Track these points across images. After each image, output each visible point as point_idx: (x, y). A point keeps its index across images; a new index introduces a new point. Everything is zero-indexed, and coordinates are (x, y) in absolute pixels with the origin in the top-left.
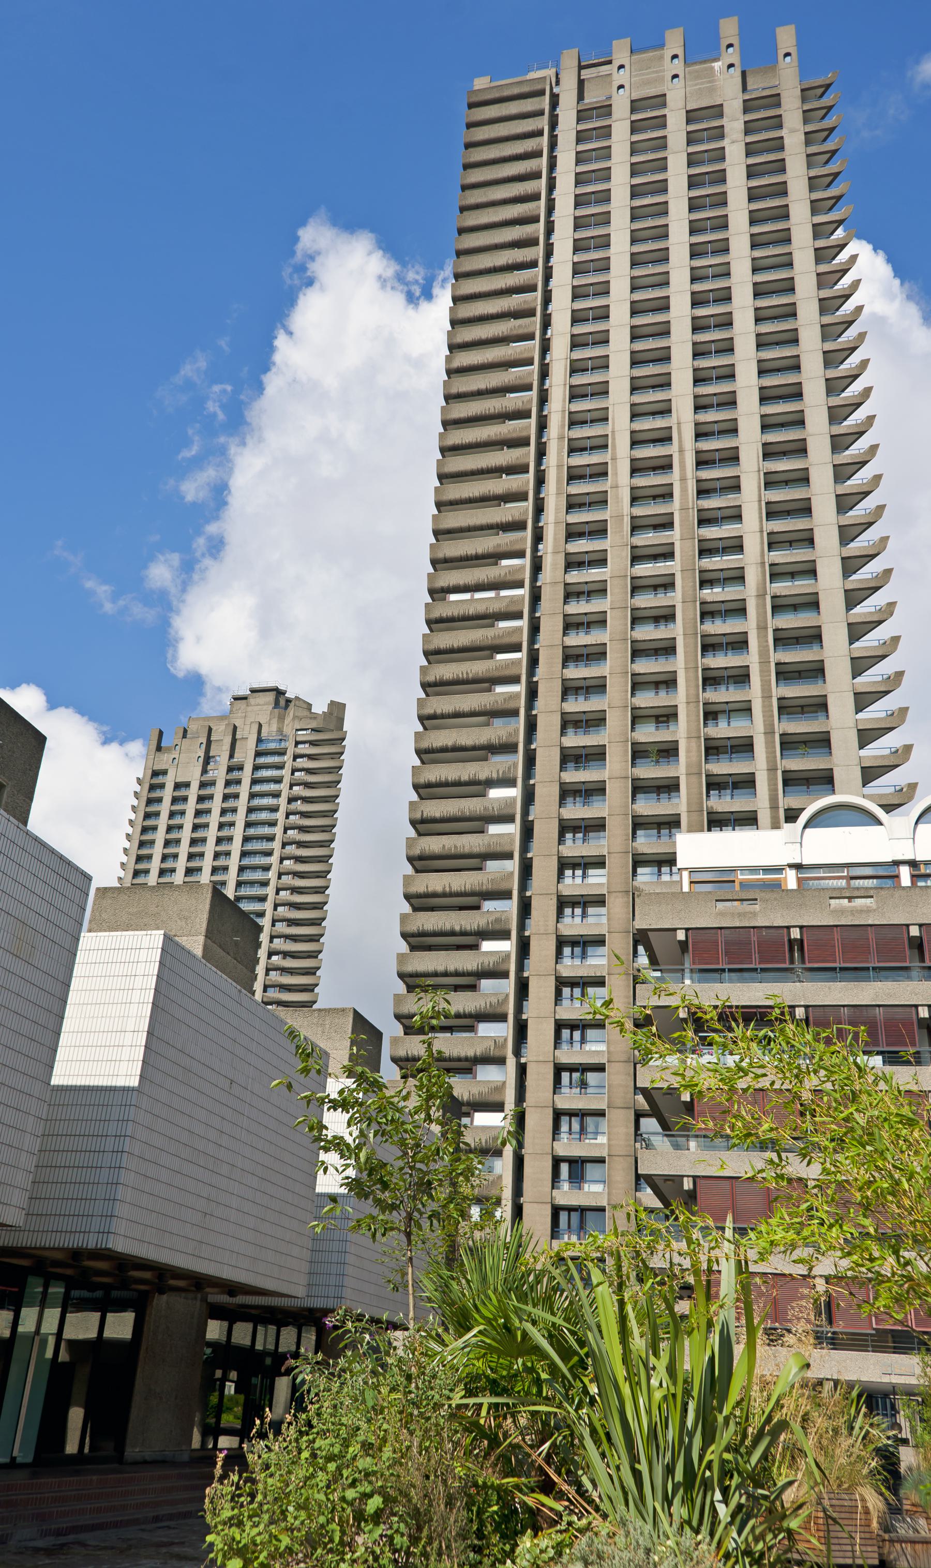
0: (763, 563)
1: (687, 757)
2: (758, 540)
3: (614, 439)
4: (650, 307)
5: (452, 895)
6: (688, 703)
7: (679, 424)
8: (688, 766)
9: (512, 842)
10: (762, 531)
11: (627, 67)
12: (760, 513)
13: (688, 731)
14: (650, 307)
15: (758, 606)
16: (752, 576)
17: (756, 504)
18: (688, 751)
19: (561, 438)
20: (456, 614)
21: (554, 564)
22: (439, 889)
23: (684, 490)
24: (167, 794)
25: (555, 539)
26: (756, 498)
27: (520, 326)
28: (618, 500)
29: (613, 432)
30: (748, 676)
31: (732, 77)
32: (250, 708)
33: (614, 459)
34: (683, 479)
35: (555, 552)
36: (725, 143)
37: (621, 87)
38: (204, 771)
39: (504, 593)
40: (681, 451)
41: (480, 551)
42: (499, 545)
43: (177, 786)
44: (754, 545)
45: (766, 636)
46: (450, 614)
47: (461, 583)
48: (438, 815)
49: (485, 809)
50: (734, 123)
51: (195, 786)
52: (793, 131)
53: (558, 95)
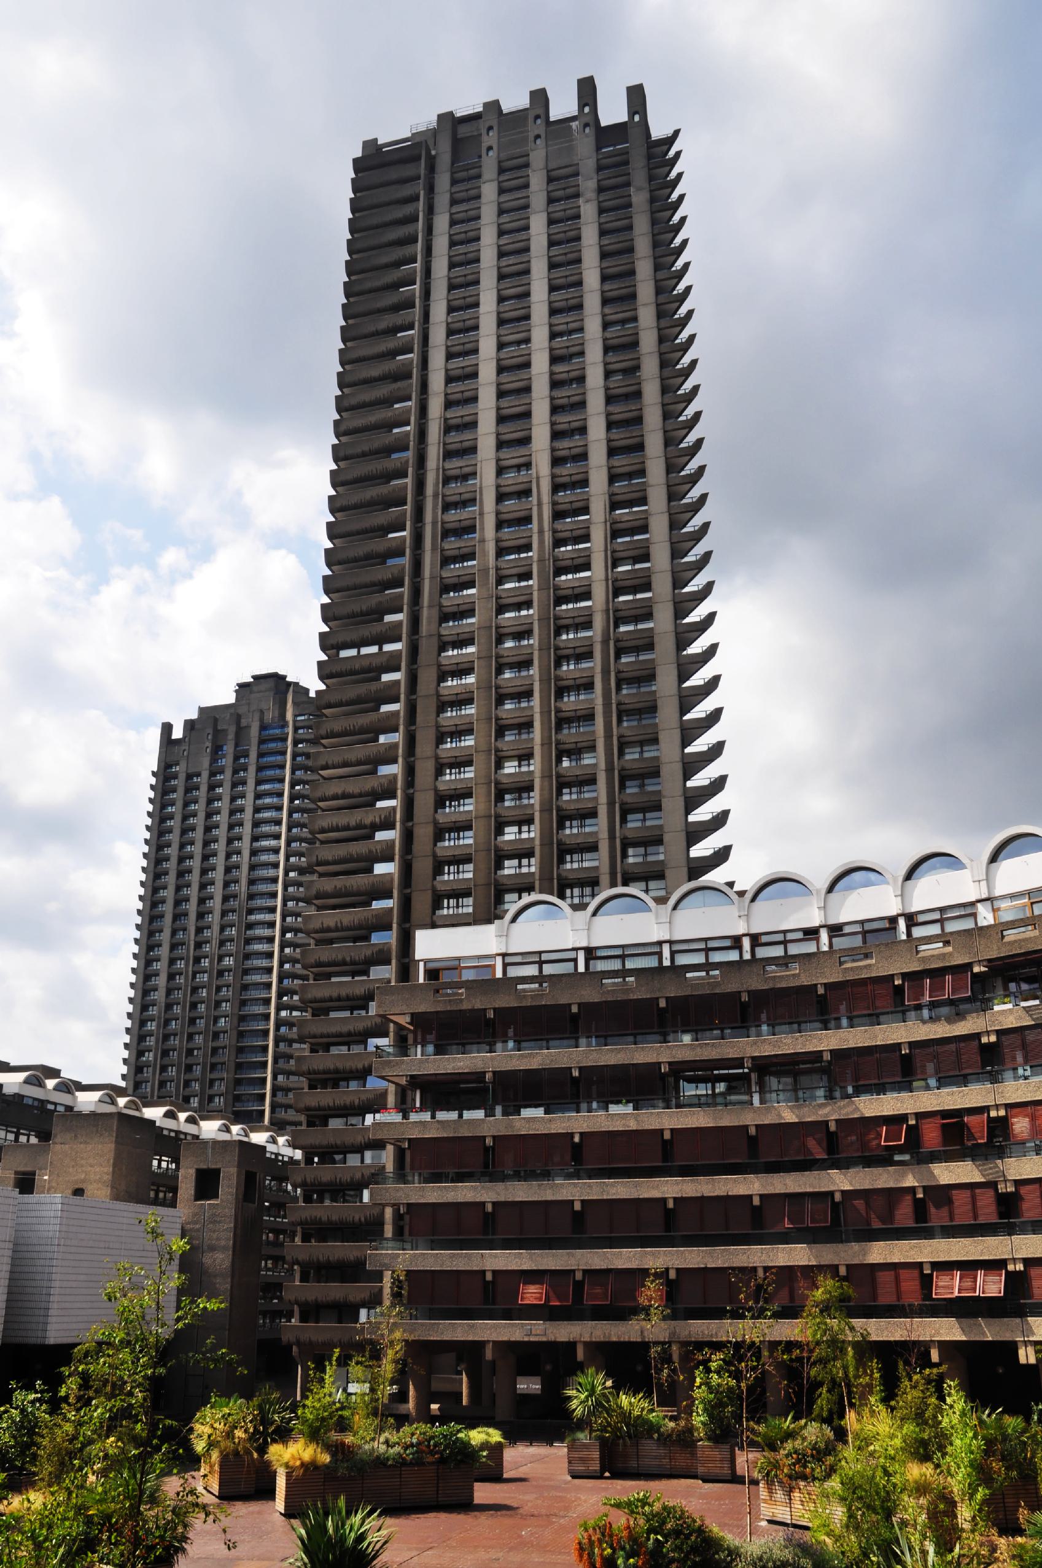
0: (607, 610)
1: (541, 795)
2: (604, 589)
3: (481, 494)
4: (514, 368)
5: (343, 929)
6: (542, 745)
7: (538, 478)
8: (542, 804)
9: (392, 880)
10: (607, 579)
11: (495, 128)
12: (606, 562)
13: (542, 771)
14: (514, 368)
15: (602, 651)
16: (598, 622)
17: (603, 554)
18: (542, 790)
19: (436, 495)
20: (344, 669)
21: (429, 618)
22: (332, 924)
23: (541, 542)
24: (179, 783)
25: (430, 593)
26: (602, 548)
27: (399, 389)
28: (485, 553)
29: (481, 488)
30: (593, 715)
31: (587, 136)
32: (253, 696)
33: (482, 514)
34: (541, 532)
35: (430, 606)
36: (581, 200)
37: (490, 148)
38: (214, 760)
39: (388, 647)
40: (540, 504)
41: (364, 608)
42: (380, 602)
43: (189, 777)
44: (599, 592)
45: (609, 680)
46: (339, 670)
47: (348, 640)
48: (330, 858)
49: (370, 851)
50: (588, 184)
51: (205, 775)
52: (639, 189)
53: (434, 157)
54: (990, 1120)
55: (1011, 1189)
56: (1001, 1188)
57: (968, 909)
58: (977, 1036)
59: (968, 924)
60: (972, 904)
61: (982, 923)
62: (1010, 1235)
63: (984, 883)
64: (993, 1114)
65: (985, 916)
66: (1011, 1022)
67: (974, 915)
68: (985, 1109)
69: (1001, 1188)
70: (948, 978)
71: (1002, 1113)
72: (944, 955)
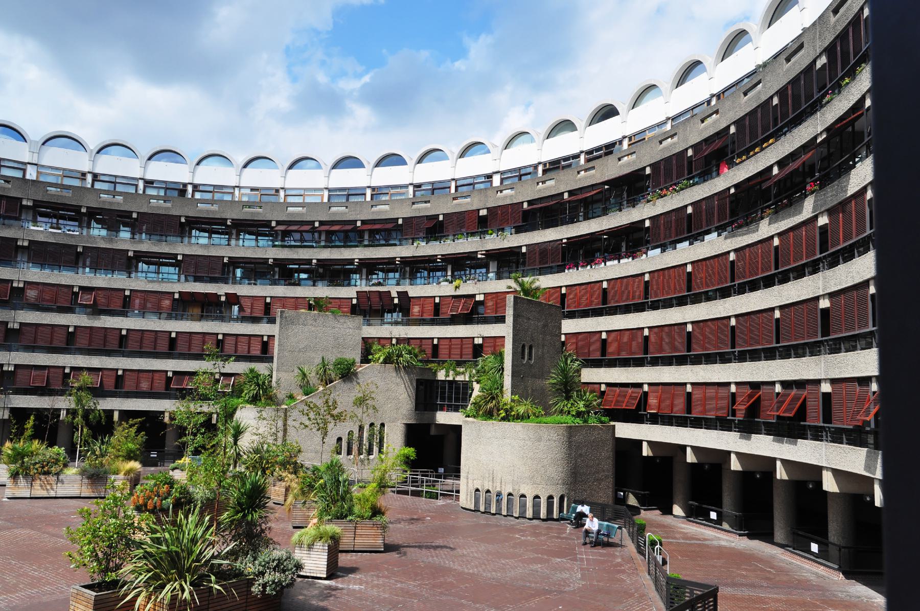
54: (13, 288)
55: (16, 326)
56: (10, 326)
57: (22, 166)
58: (16, 240)
59: (18, 174)
60: (25, 164)
61: (28, 177)
62: (10, 351)
63: (36, 155)
64: (15, 285)
65: (31, 174)
66: (41, 238)
67: (24, 171)
68: (12, 281)
69: (10, 326)
70: (4, 202)
71: (21, 285)
72: (4, 188)
